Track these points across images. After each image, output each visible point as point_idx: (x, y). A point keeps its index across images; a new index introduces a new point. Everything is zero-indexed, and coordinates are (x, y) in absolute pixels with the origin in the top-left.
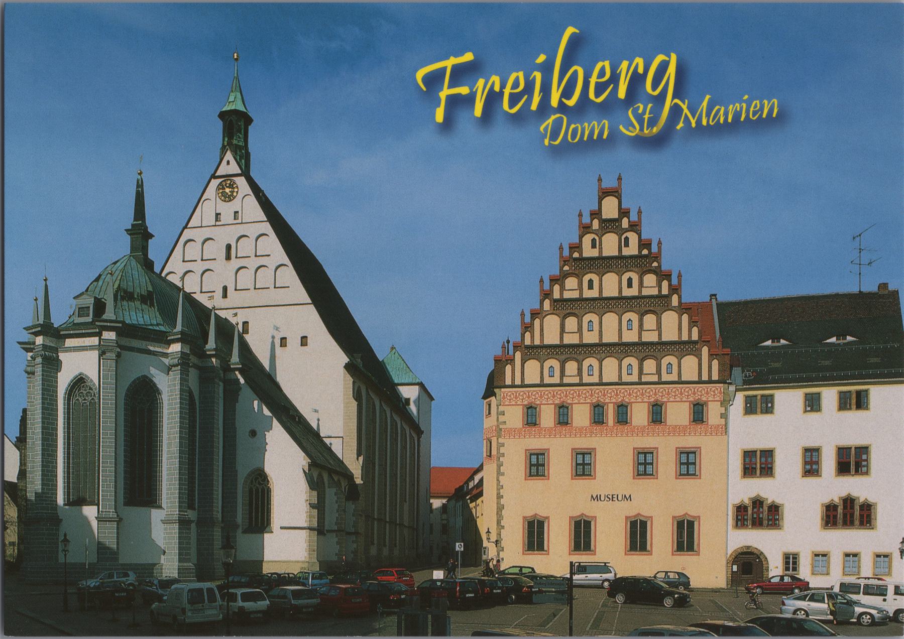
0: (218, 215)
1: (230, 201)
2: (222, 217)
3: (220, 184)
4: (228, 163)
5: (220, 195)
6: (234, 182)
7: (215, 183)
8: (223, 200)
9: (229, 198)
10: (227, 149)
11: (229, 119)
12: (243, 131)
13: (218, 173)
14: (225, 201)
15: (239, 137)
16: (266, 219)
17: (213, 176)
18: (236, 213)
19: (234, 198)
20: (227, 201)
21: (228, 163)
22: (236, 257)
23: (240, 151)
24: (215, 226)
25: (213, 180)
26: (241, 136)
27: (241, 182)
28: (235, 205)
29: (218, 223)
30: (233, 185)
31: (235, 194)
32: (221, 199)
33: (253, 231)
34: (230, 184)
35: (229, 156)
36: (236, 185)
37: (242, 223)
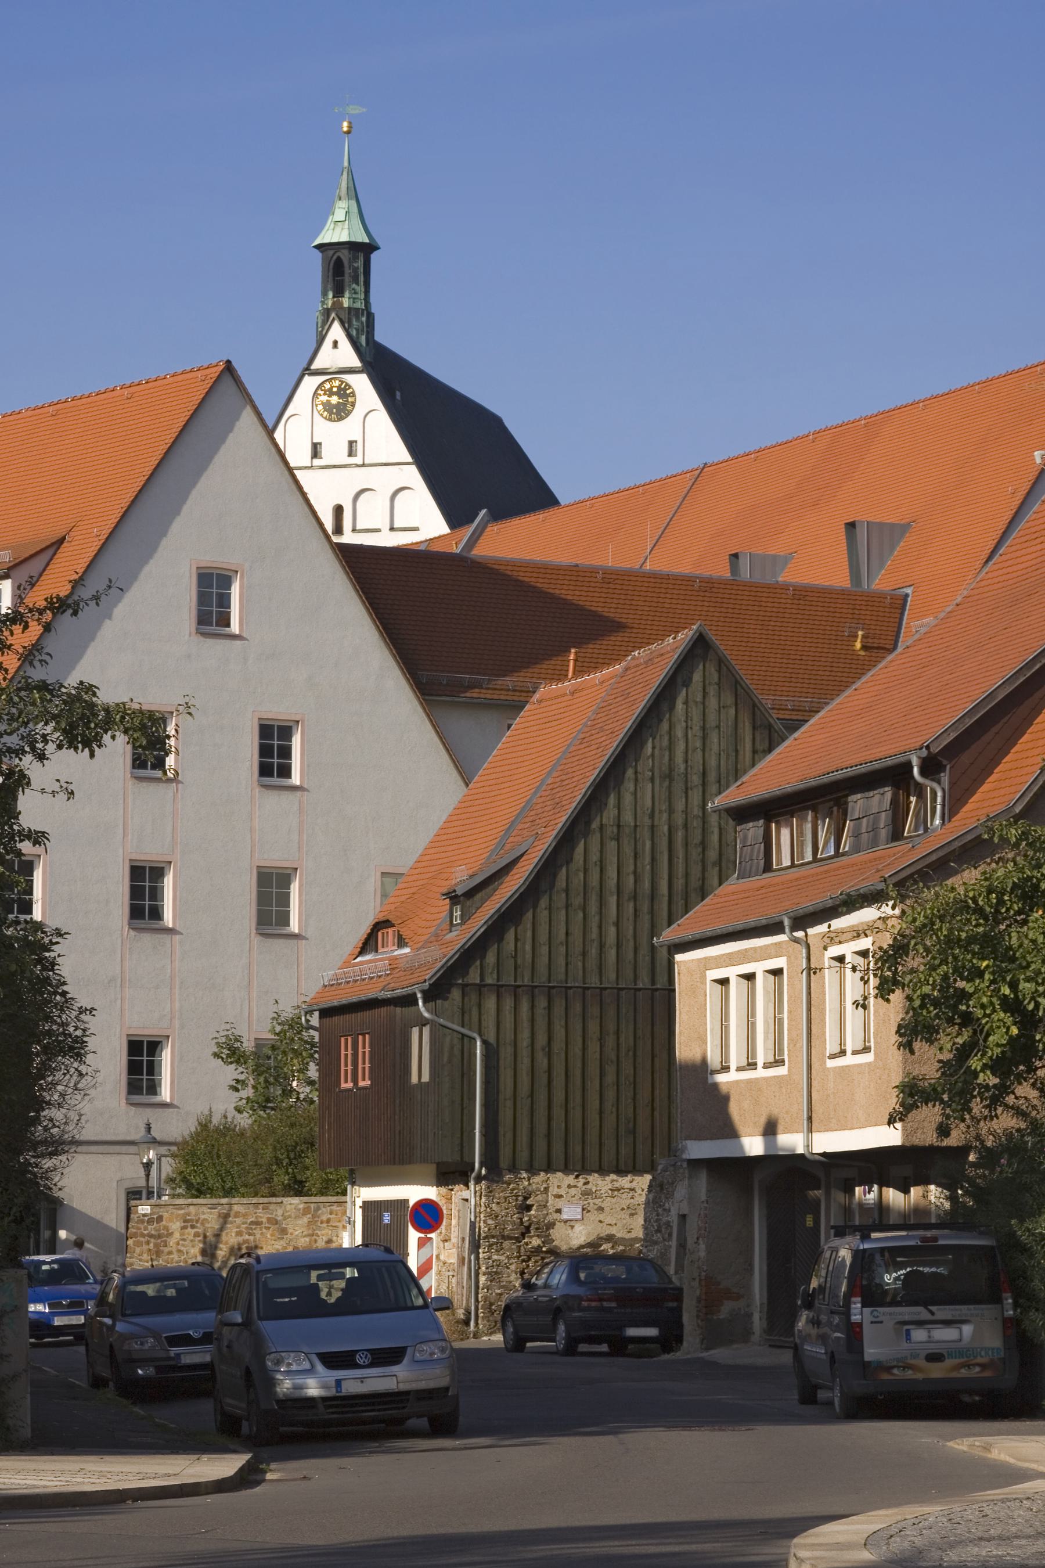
0: (316, 450)
1: (340, 419)
2: (324, 451)
3: (320, 386)
4: (335, 344)
5: (320, 407)
6: (347, 384)
7: (310, 383)
8: (325, 418)
9: (339, 412)
10: (334, 319)
11: (335, 257)
12: (362, 279)
13: (315, 366)
14: (330, 420)
15: (356, 293)
16: (410, 459)
17: (308, 371)
18: (351, 443)
19: (347, 415)
20: (335, 421)
21: (335, 344)
22: (354, 530)
23: (358, 319)
24: (311, 467)
25: (306, 377)
26: (358, 288)
27: (362, 386)
28: (350, 427)
29: (317, 462)
30: (345, 389)
31: (349, 407)
32: (322, 415)
33: (385, 480)
34: (339, 387)
35: (336, 331)
36: (351, 390)
37: (363, 465)
